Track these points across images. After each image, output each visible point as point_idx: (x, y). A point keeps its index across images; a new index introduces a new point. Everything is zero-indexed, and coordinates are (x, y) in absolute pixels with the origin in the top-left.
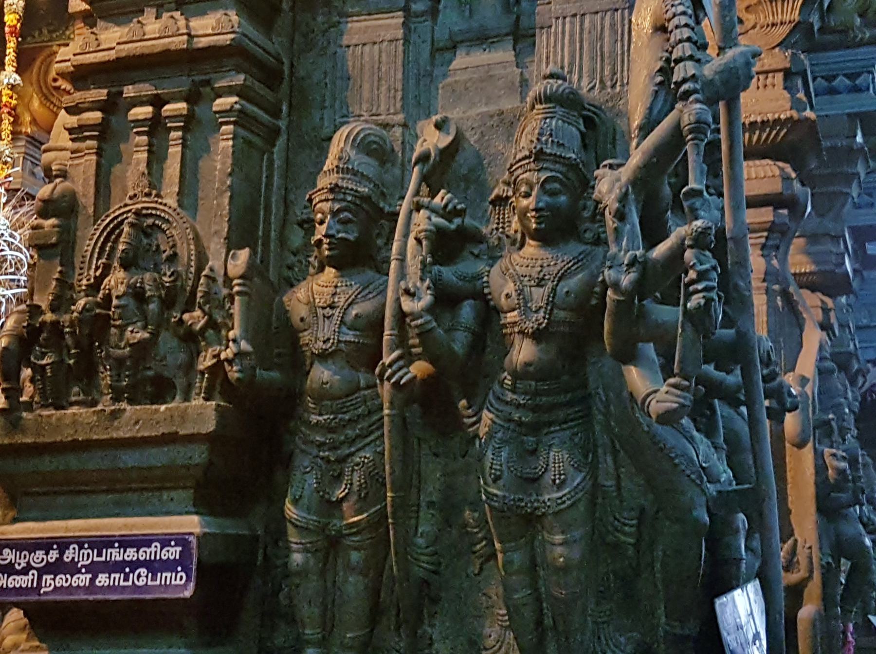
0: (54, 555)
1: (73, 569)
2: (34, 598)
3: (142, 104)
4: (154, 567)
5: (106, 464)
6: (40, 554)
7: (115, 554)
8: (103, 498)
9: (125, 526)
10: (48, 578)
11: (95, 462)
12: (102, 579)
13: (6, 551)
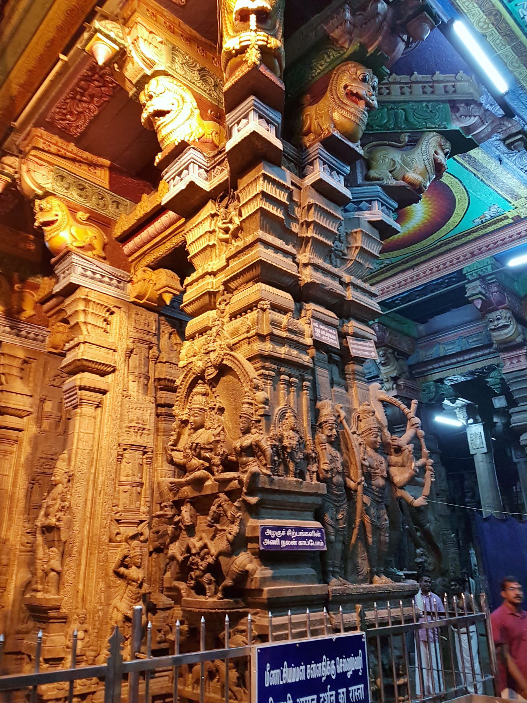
0: (284, 533)
1: (290, 538)
2: (280, 549)
3: (285, 375)
4: (315, 539)
5: (295, 501)
6: (279, 532)
7: (302, 534)
8: (287, 512)
9: (302, 524)
10: (283, 541)
11: (292, 499)
12: (301, 543)
13: (268, 530)
